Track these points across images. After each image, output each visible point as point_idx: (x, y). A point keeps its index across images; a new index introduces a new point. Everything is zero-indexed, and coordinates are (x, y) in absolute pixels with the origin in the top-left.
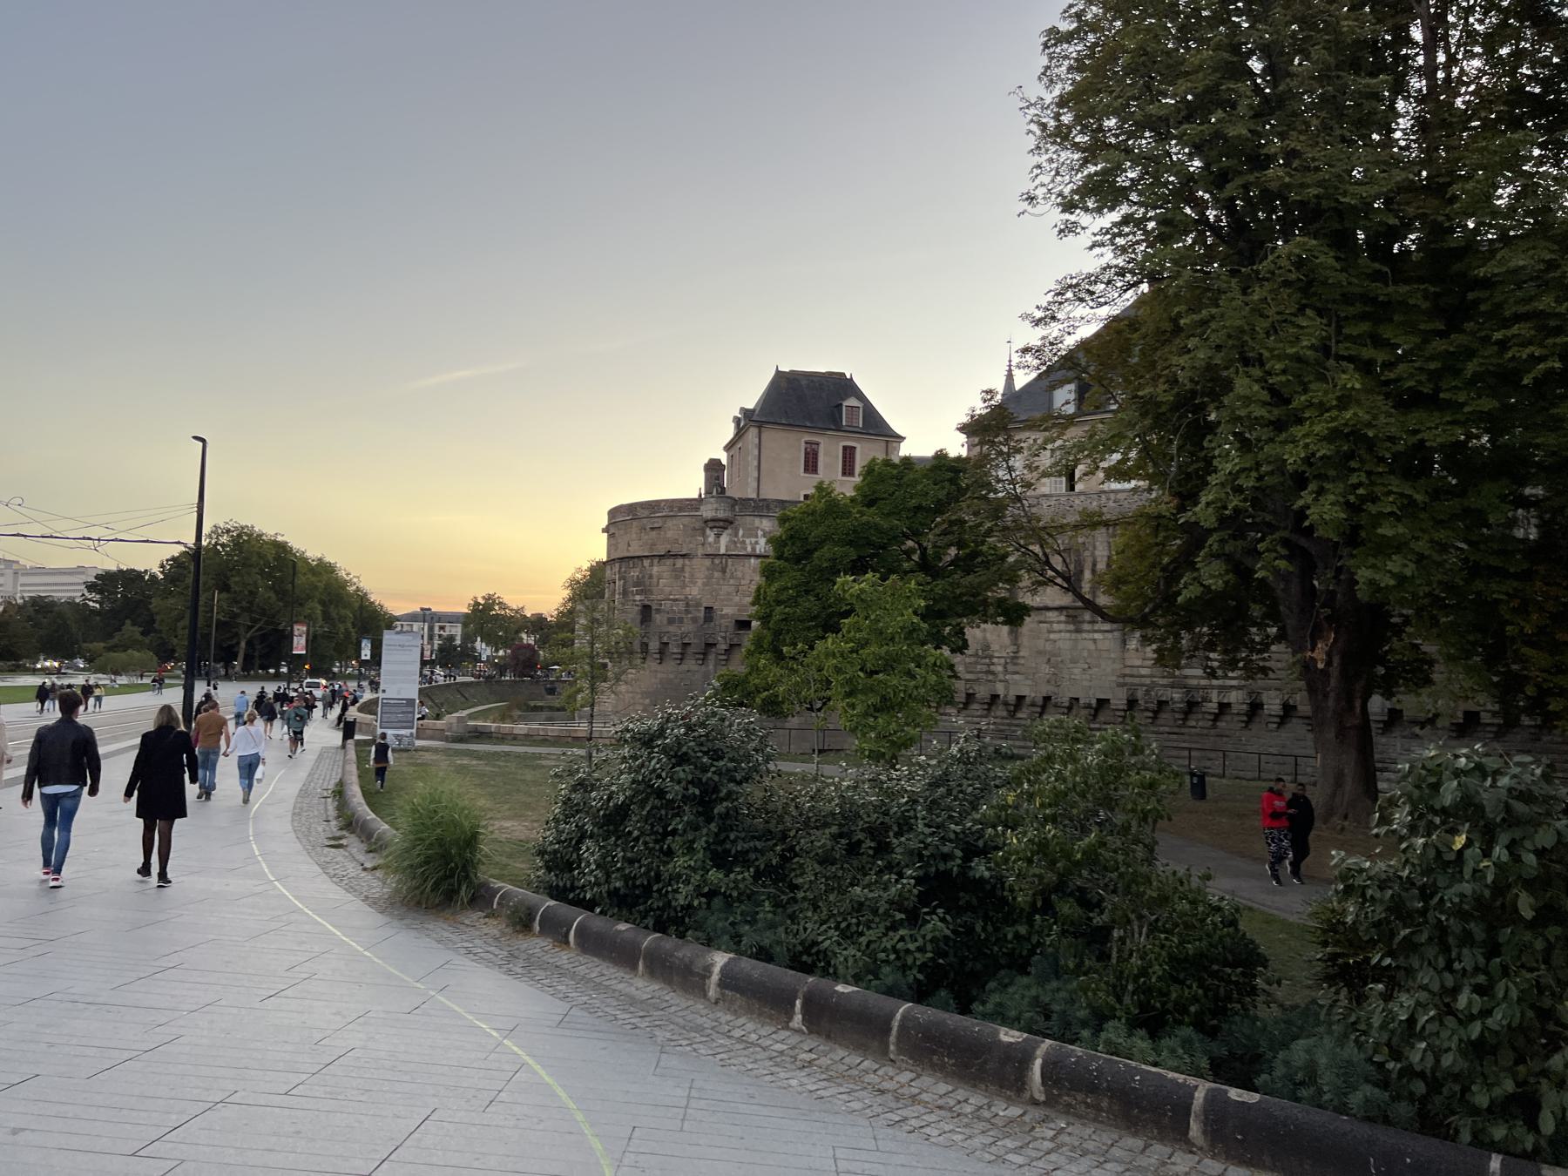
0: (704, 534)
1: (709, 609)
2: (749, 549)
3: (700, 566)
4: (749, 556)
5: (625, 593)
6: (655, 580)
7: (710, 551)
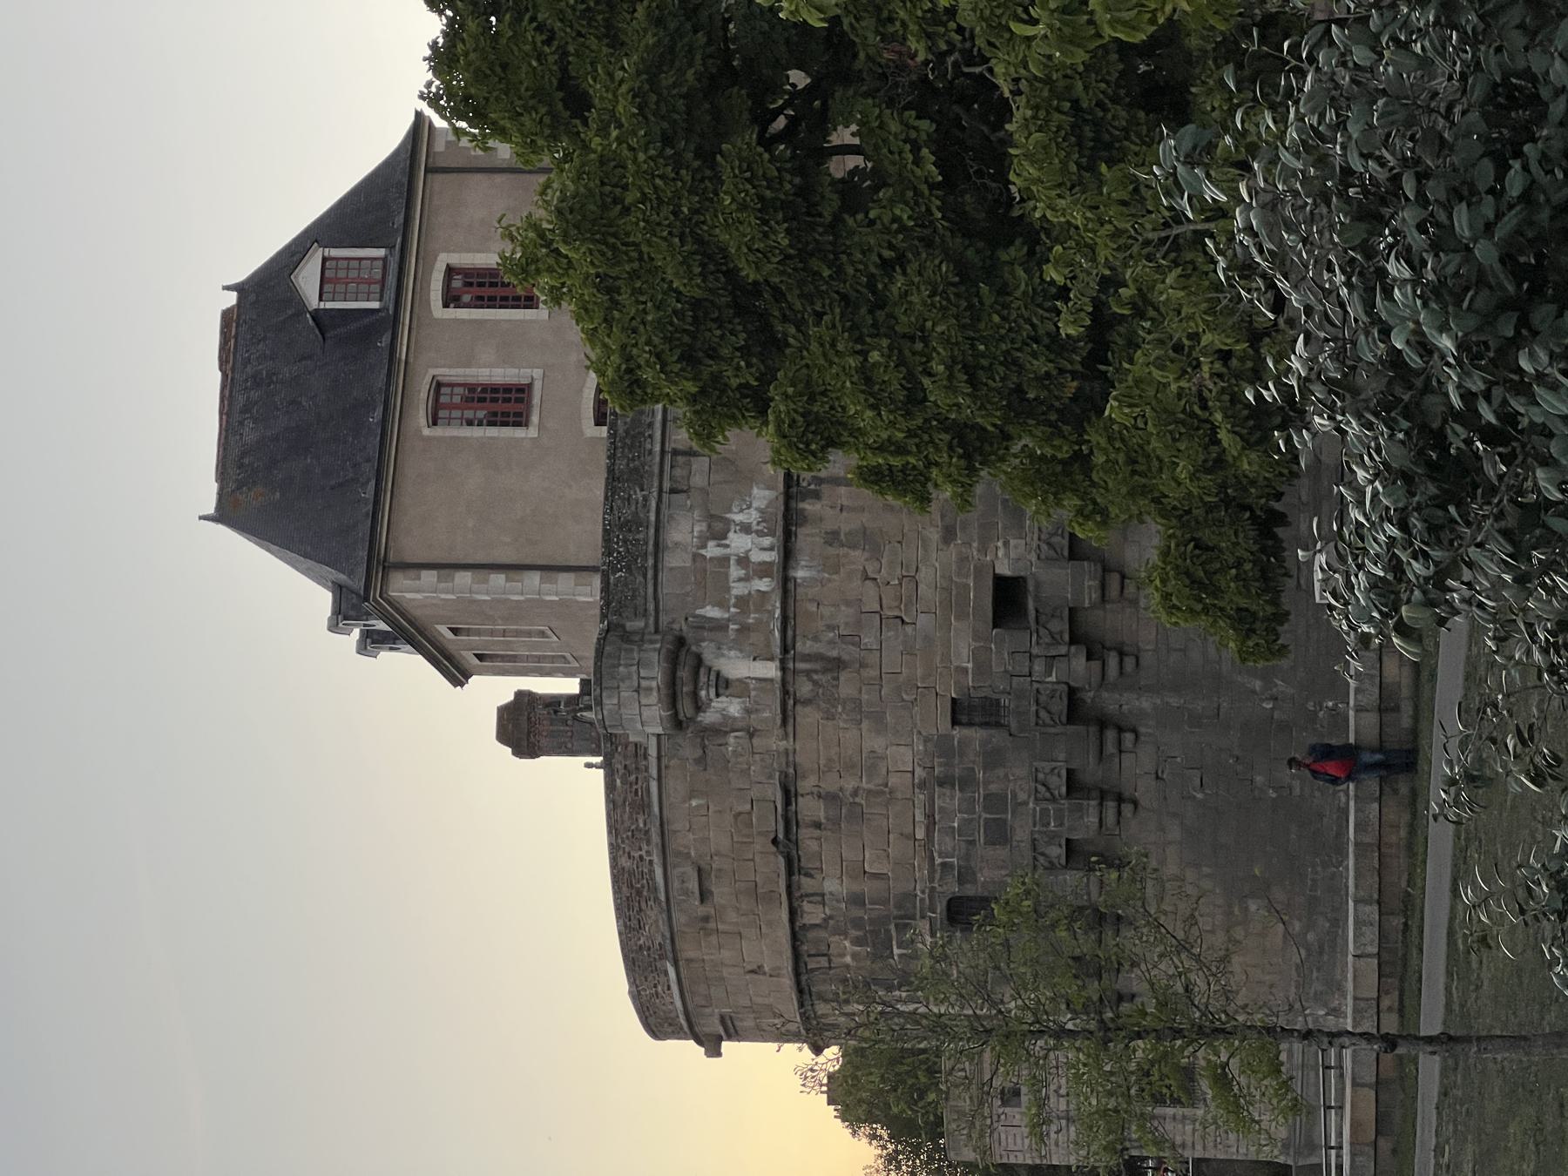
0: (718, 731)
1: (959, 712)
2: (763, 585)
4: (786, 585)
6: (868, 888)
7: (770, 712)
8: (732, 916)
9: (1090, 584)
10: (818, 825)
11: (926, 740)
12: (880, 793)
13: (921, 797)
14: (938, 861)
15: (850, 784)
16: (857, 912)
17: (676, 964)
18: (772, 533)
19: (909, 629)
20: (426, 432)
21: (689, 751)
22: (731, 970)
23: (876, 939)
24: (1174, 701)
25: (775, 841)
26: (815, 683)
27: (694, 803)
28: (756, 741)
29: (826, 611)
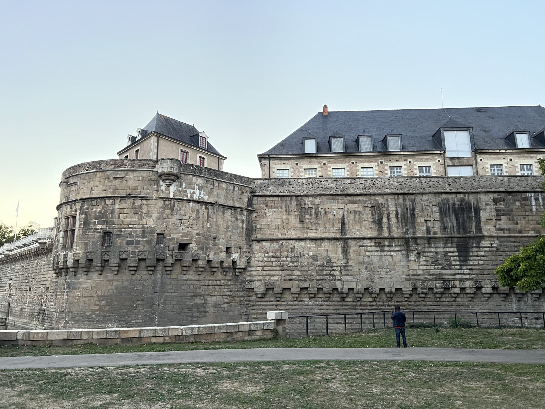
0: (158, 184)
3: (155, 206)
4: (189, 201)
5: (86, 223)
6: (116, 214)
7: (162, 195)
8: (110, 184)
9: (187, 264)
10: (134, 204)
11: (154, 228)
12: (142, 218)
13: (140, 226)
14: (123, 230)
15: (144, 211)
16: (109, 212)
17: (96, 172)
18: (199, 199)
19: (179, 225)
20: (180, 149)
21: (153, 177)
22: (92, 184)
23: (100, 216)
24: (159, 283)
25: (129, 194)
26: (168, 205)
27: (140, 177)
28: (155, 192)
29: (184, 208)
